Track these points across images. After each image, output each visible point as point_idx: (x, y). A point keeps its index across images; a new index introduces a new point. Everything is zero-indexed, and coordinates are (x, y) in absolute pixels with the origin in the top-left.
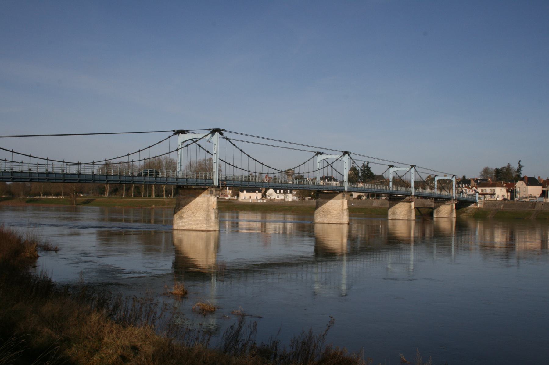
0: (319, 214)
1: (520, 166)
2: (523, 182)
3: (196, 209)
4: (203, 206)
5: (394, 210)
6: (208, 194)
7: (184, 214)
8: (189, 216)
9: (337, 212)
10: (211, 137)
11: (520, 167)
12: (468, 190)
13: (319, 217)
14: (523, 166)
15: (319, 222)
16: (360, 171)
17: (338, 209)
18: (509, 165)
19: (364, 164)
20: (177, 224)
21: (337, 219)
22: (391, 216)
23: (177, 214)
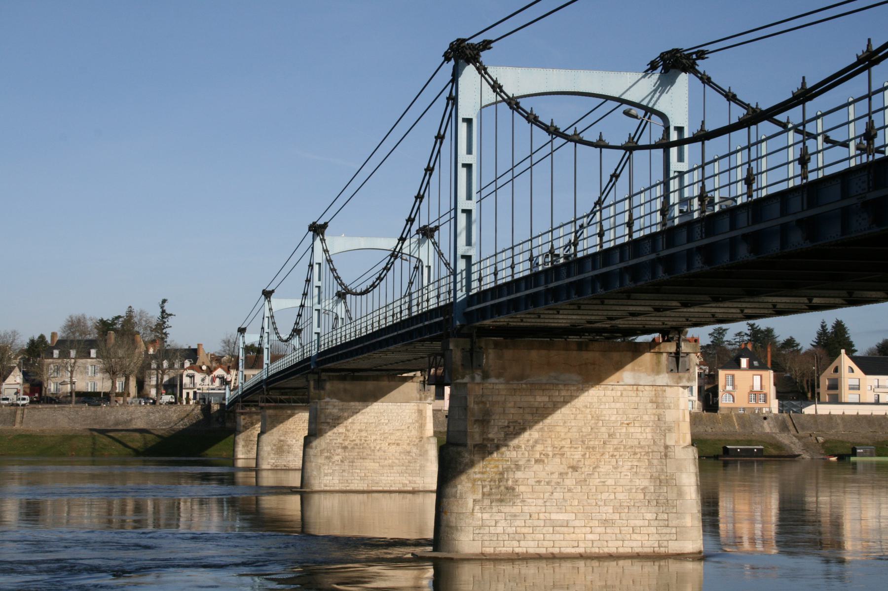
0: (328, 458)
1: (164, 315)
3: (593, 448)
4: (631, 430)
5: (282, 438)
6: (656, 370)
7: (519, 475)
8: (548, 483)
9: (399, 449)
10: (655, 91)
11: (163, 317)
12: (198, 377)
13: (326, 469)
14: (171, 315)
15: (328, 488)
17: (405, 437)
18: (130, 311)
20: (481, 527)
21: (401, 473)
22: (272, 459)
23: (476, 472)
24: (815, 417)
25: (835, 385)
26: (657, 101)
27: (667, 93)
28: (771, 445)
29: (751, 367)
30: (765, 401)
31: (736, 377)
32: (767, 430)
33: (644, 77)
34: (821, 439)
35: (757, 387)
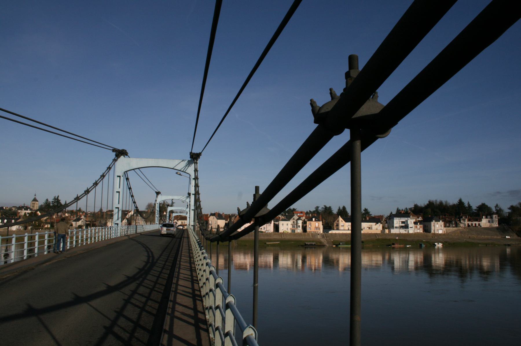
2: (214, 217)
10: (186, 166)
11: (172, 203)
14: (174, 203)
16: (51, 203)
19: (55, 197)
24: (332, 234)
25: (338, 225)
26: (186, 170)
27: (190, 167)
28: (319, 242)
29: (315, 220)
30: (319, 229)
31: (312, 223)
32: (319, 237)
33: (182, 161)
34: (332, 240)
35: (317, 226)
